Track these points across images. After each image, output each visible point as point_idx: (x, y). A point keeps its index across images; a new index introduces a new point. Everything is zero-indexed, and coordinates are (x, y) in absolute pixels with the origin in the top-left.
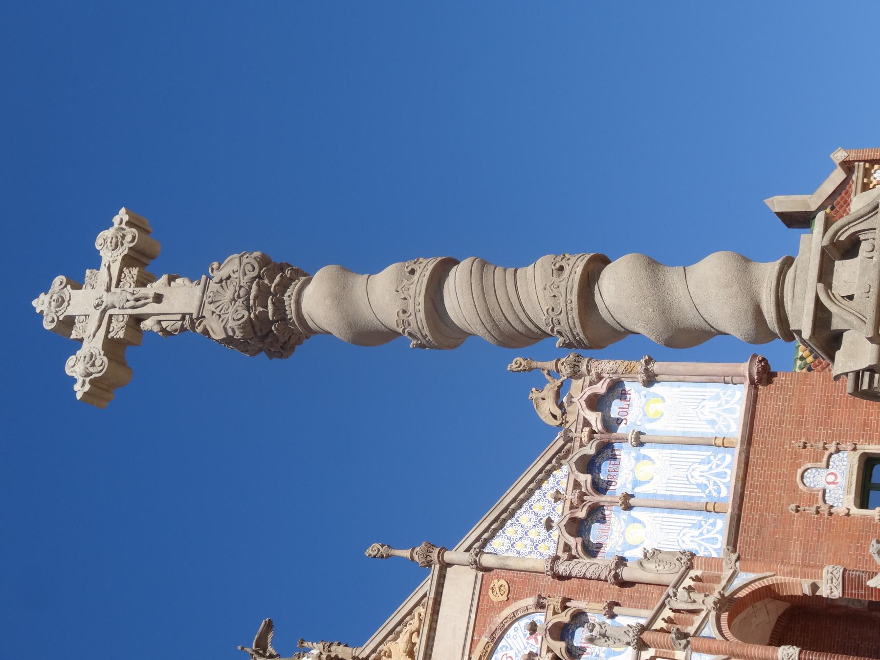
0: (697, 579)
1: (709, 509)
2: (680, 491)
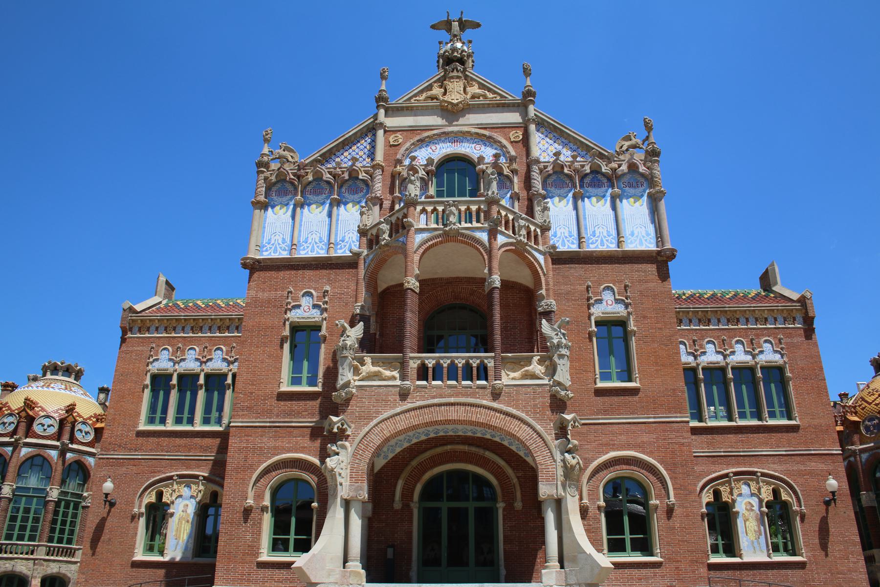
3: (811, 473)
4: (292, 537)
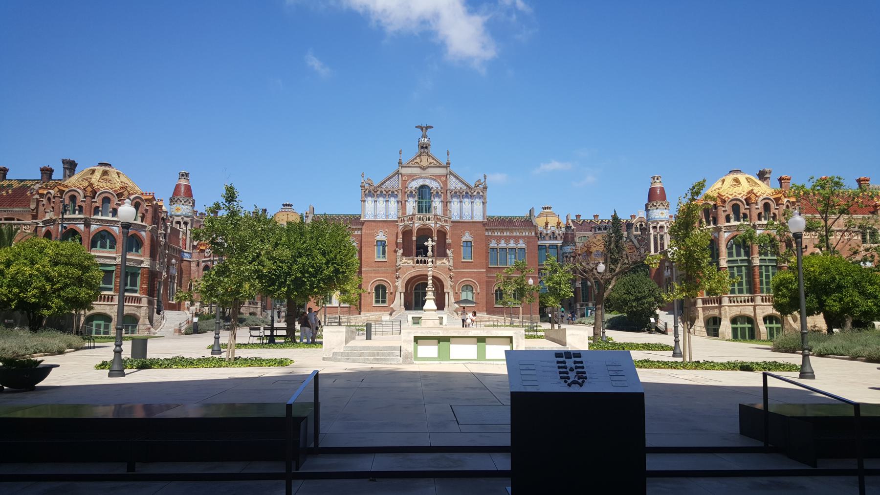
0: (447, 220)
1: (461, 217)
4: (380, 300)
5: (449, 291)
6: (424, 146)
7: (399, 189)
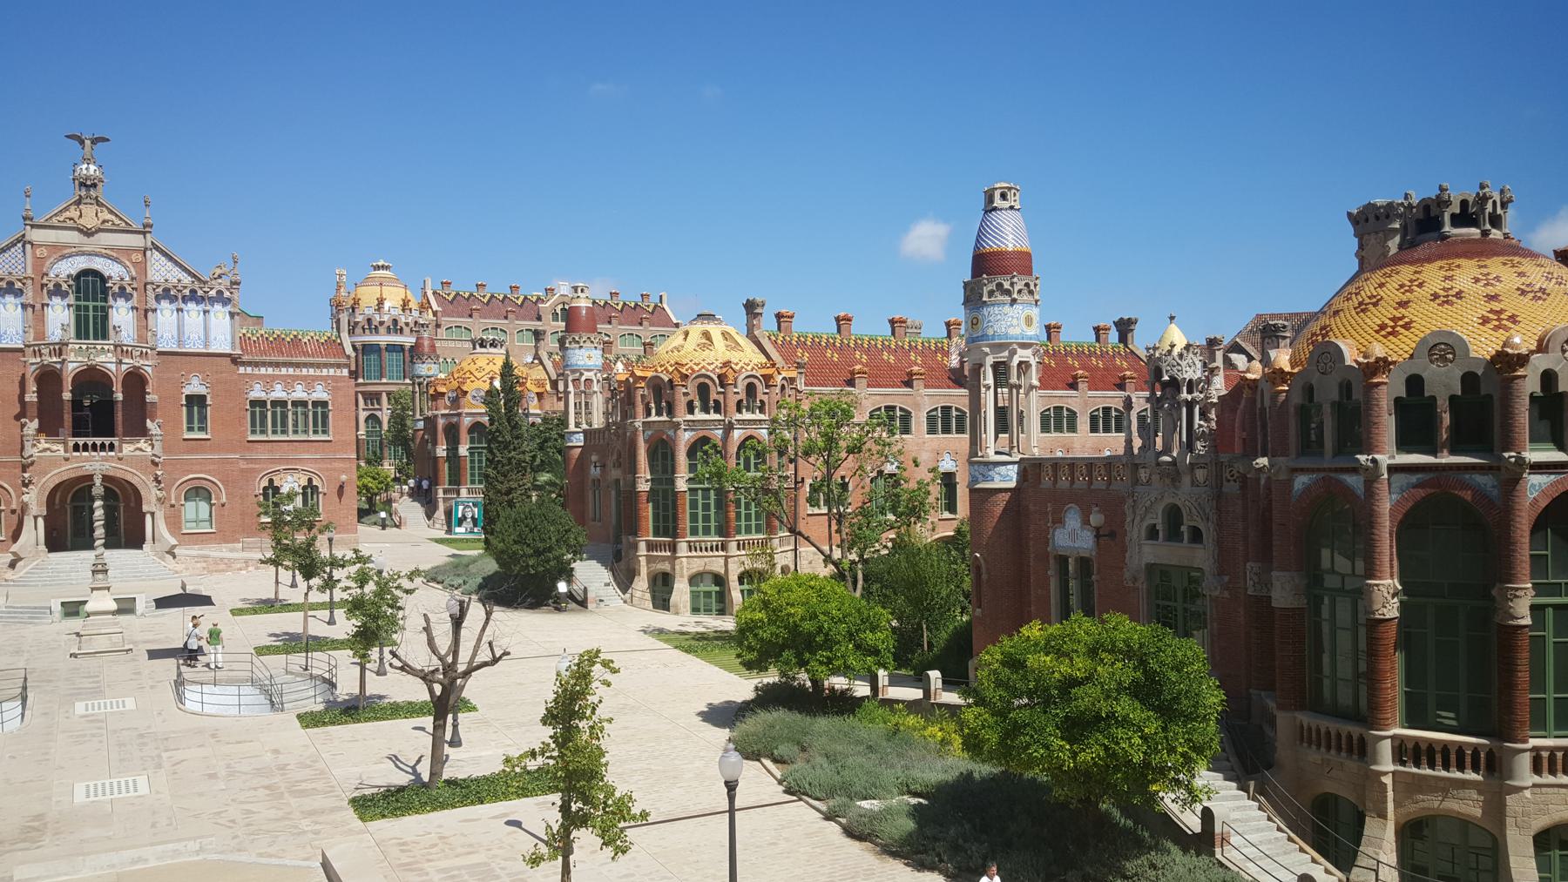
0: (147, 353)
1: (180, 342)
2: (187, 329)
3: (334, 470)
5: (154, 510)
6: (89, 183)
7: (25, 278)
